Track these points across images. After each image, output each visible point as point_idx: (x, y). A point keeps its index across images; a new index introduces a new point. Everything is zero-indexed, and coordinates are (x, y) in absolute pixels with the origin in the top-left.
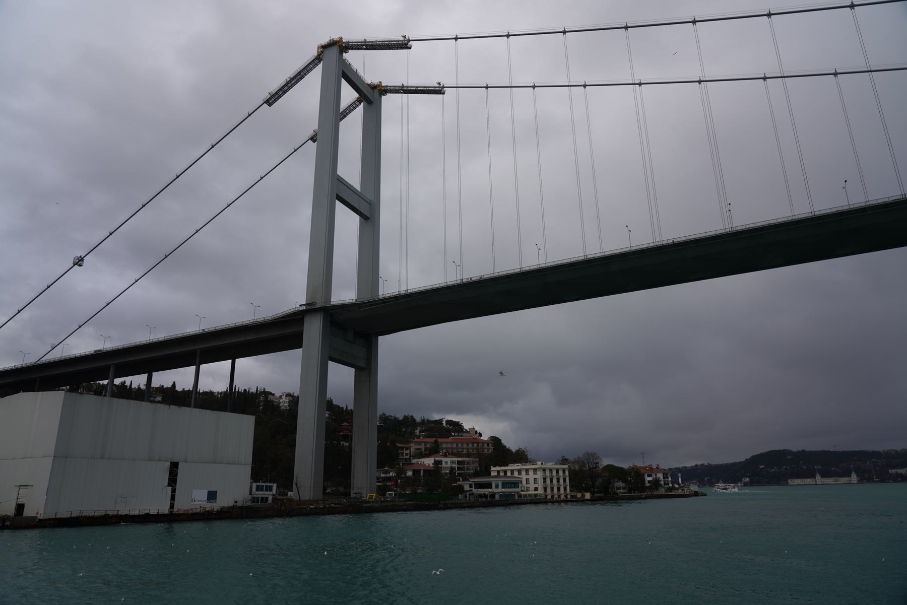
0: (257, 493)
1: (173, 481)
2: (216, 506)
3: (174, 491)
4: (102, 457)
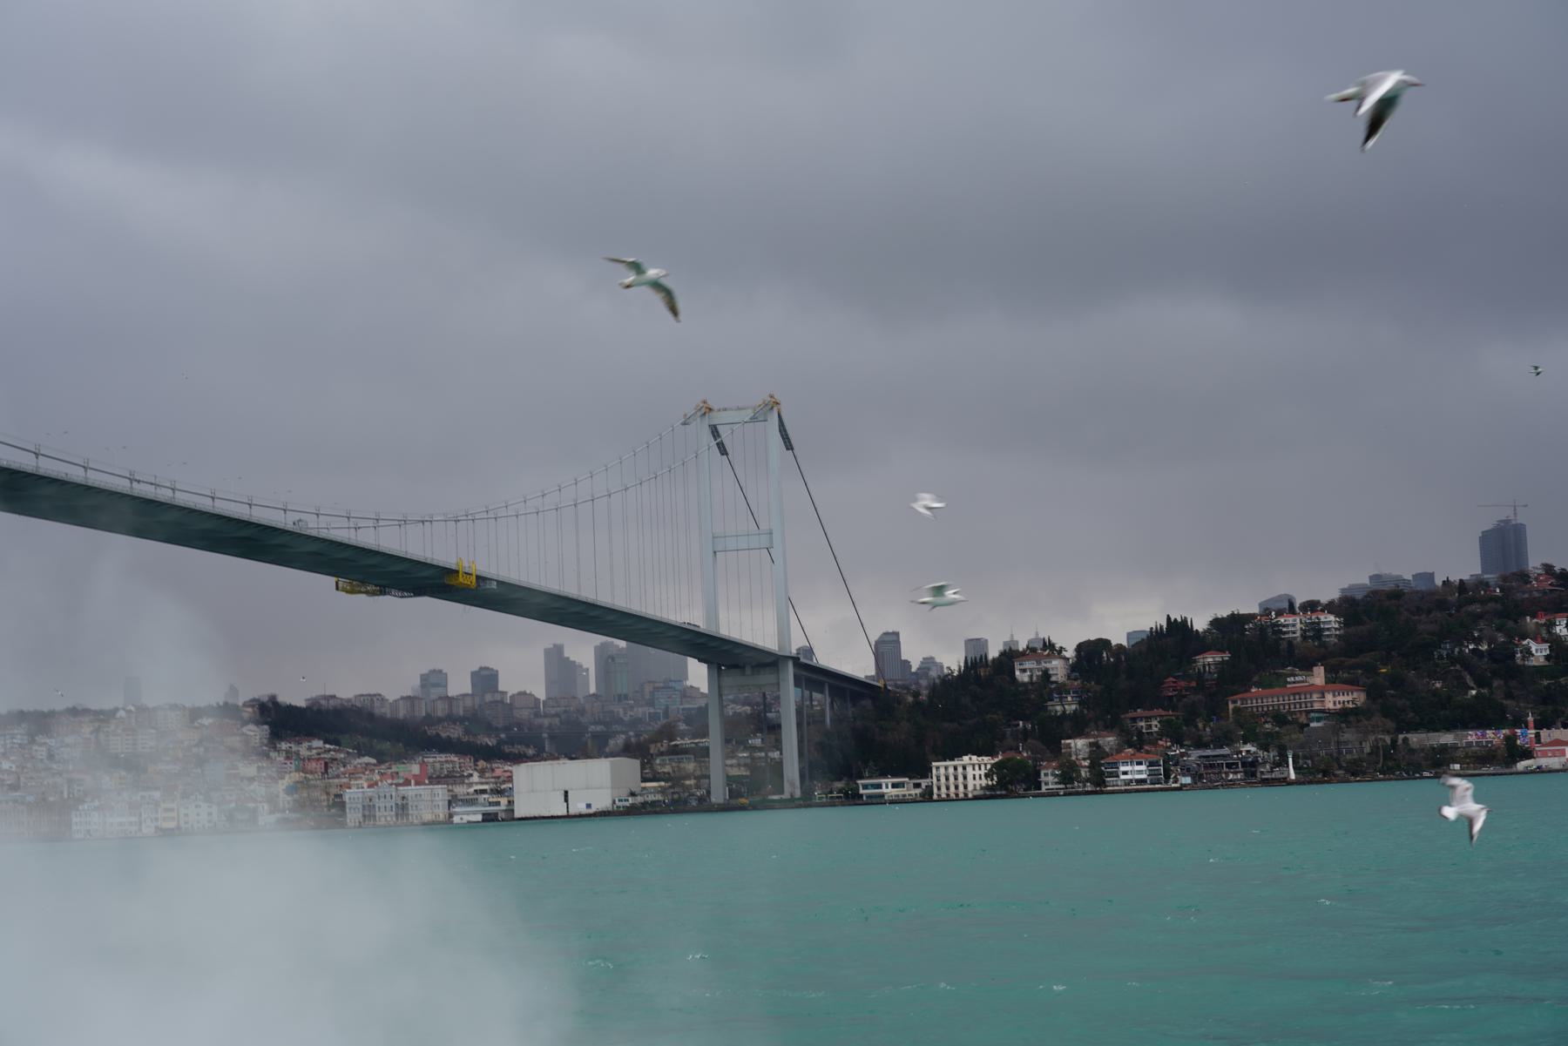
1: (566, 800)
2: (591, 811)
3: (568, 805)
4: (533, 791)
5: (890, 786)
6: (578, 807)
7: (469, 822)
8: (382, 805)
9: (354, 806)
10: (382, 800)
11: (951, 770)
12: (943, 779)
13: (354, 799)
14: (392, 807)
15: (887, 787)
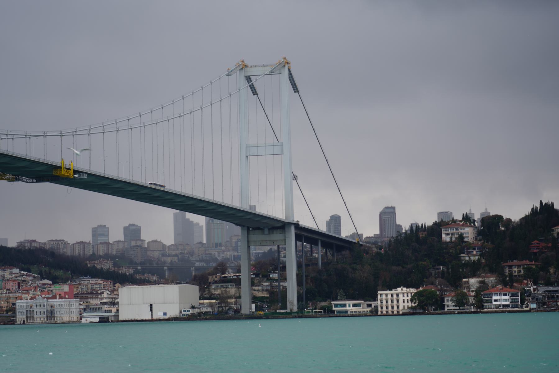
0: (184, 313)
1: (151, 310)
2: (167, 317)
3: (152, 313)
4: (131, 304)
5: (351, 306)
6: (158, 314)
7: (91, 322)
8: (38, 311)
9: (21, 311)
10: (38, 307)
11: (389, 296)
12: (384, 302)
13: (21, 306)
14: (44, 312)
15: (350, 306)
